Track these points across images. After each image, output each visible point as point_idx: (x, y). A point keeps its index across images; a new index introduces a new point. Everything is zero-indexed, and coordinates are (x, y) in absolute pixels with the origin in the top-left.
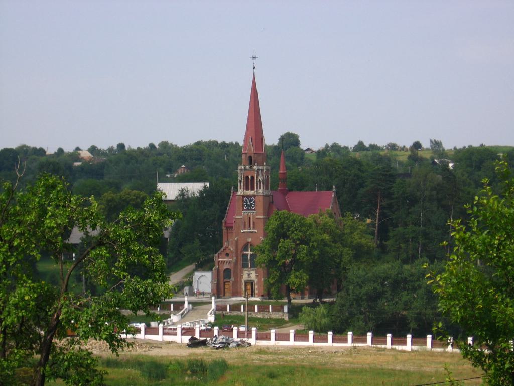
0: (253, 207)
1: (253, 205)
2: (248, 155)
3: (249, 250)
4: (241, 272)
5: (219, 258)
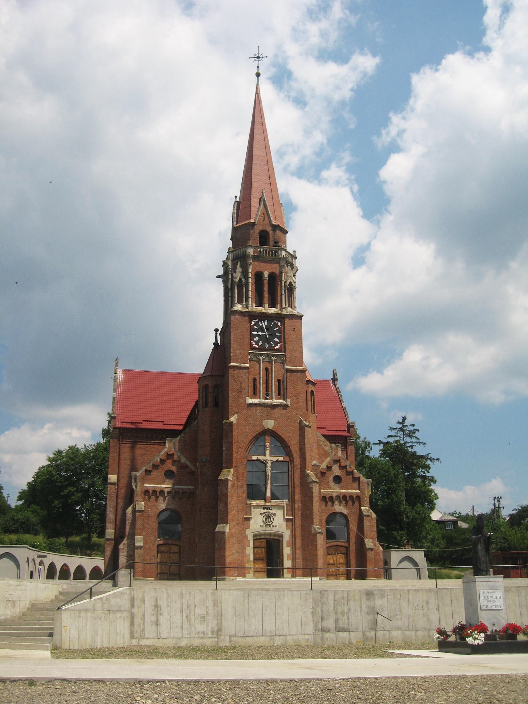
0: (276, 344)
1: (276, 340)
2: (258, 229)
4: (247, 510)
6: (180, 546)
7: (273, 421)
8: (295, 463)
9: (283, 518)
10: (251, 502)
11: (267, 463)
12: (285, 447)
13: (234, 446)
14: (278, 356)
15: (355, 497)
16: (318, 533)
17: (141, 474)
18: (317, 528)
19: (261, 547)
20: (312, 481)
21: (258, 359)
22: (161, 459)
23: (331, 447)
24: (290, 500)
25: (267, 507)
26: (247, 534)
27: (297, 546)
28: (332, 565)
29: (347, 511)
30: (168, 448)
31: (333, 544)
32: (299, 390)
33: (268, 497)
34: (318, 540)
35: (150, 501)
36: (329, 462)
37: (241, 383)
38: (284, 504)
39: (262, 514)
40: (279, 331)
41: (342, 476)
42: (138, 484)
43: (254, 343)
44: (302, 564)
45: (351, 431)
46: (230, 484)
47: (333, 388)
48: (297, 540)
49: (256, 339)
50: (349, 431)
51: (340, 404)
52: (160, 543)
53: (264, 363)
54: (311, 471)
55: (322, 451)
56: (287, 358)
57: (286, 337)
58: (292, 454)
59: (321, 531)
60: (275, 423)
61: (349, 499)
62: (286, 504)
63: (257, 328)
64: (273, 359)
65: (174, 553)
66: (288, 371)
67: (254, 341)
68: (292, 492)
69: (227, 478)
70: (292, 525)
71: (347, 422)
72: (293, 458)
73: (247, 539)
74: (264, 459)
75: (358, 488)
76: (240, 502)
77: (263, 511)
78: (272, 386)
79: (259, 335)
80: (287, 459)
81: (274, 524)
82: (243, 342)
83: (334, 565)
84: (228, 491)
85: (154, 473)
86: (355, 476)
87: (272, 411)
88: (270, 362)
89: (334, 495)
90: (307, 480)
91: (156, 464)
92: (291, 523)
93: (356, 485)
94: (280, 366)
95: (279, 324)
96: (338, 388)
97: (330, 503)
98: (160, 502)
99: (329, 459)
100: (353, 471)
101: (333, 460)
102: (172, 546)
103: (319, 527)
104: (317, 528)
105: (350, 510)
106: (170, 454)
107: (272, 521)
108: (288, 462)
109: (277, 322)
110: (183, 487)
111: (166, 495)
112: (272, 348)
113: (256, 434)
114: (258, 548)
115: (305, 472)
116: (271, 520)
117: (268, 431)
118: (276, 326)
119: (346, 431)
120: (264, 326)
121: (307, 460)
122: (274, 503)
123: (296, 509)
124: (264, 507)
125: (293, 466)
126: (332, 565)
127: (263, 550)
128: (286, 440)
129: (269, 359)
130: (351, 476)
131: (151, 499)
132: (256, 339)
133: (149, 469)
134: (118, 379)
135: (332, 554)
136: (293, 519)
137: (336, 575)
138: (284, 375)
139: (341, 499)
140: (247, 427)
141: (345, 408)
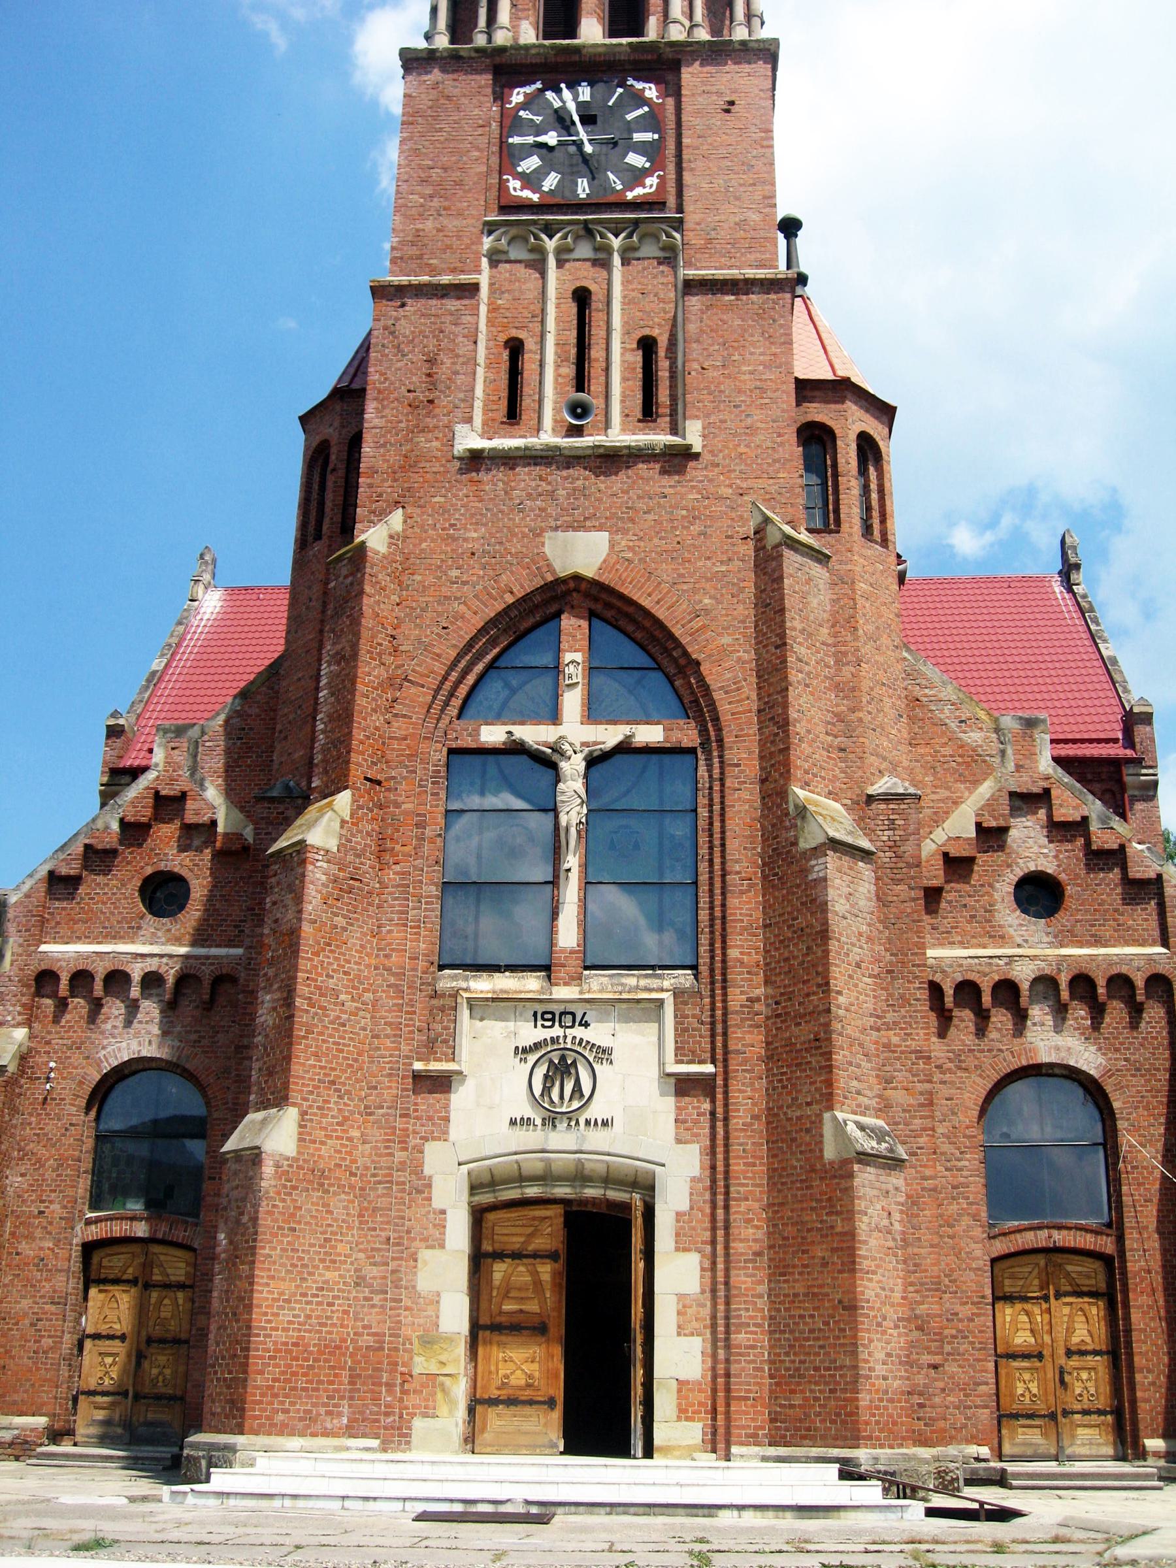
0: (637, 177)
1: (636, 160)
3: (572, 702)
5: (41, 928)
6: (194, 1250)
7: (605, 535)
8: (728, 755)
9: (654, 1073)
10: (464, 985)
11: (562, 754)
12: (672, 670)
13: (362, 670)
14: (643, 228)
15: (1139, 982)
16: (864, 1158)
17: (27, 896)
18: (862, 1128)
19: (535, 1255)
20: (821, 839)
21: (532, 250)
22: (127, 819)
23: (997, 730)
24: (704, 969)
25: (557, 1008)
26: (427, 1171)
27: (738, 1247)
28: (1026, 1356)
29: (1101, 1060)
30: (161, 768)
31: (1030, 1239)
32: (751, 373)
33: (563, 951)
34: (860, 1205)
35: (63, 1023)
36: (990, 805)
37: (431, 361)
38: (662, 990)
39: (525, 1051)
40: (653, 121)
41: (1063, 877)
42: (11, 940)
43: (514, 184)
44: (771, 1362)
45: (1137, 740)
46: (317, 875)
47: (1064, 599)
48: (739, 1209)
49: (531, 163)
50: (1129, 742)
51: (1092, 649)
52: (95, 1233)
53: (567, 265)
54: (830, 794)
55: (947, 751)
56: (689, 235)
57: (686, 141)
58: (712, 704)
59: (891, 1150)
60: (612, 545)
61: (1110, 996)
62: (678, 993)
63: (538, 119)
64: (616, 242)
65: (167, 1286)
66: (691, 286)
67: (523, 177)
68: (712, 919)
69: (299, 837)
70: (713, 1113)
71: (1115, 701)
72: (719, 730)
73: (430, 1199)
74: (552, 739)
75: (1156, 934)
76: (392, 980)
77: (531, 1033)
78: (607, 370)
79: (544, 146)
80: (688, 736)
81: (596, 1111)
82: (459, 183)
83: (1040, 1356)
84: (300, 911)
85: (94, 887)
86: (1135, 872)
87: (603, 483)
88: (603, 263)
89: (1023, 974)
90: (795, 844)
91: (99, 847)
92: (706, 1106)
93: (1144, 917)
94: (662, 282)
95: (651, 92)
96: (1084, 596)
97: (1001, 1019)
98: (109, 1026)
99: (986, 789)
100: (1122, 847)
101: (1013, 795)
102: (156, 1249)
103: (880, 1123)
104: (862, 1128)
105: (1117, 1050)
106: (172, 793)
107: (587, 1091)
108: (692, 751)
109: (639, 85)
110: (222, 951)
111: (135, 992)
112: (612, 199)
113: (499, 607)
114: (517, 1256)
115: (783, 793)
116: (577, 1082)
117: (576, 590)
118: (639, 99)
119: (1116, 741)
120: (572, 106)
121: (798, 730)
122: (599, 984)
123: (733, 1020)
124: (540, 1008)
125: (722, 773)
126: (1026, 1356)
127: (546, 1271)
128: (677, 631)
129: (596, 249)
130: (1115, 875)
131: (68, 1017)
132: (531, 163)
133: (64, 871)
134: (198, 617)
135: (1025, 1299)
136: (719, 1082)
137: (1053, 1416)
138: (675, 317)
139: (1065, 995)
140: (454, 573)
141: (1114, 661)
